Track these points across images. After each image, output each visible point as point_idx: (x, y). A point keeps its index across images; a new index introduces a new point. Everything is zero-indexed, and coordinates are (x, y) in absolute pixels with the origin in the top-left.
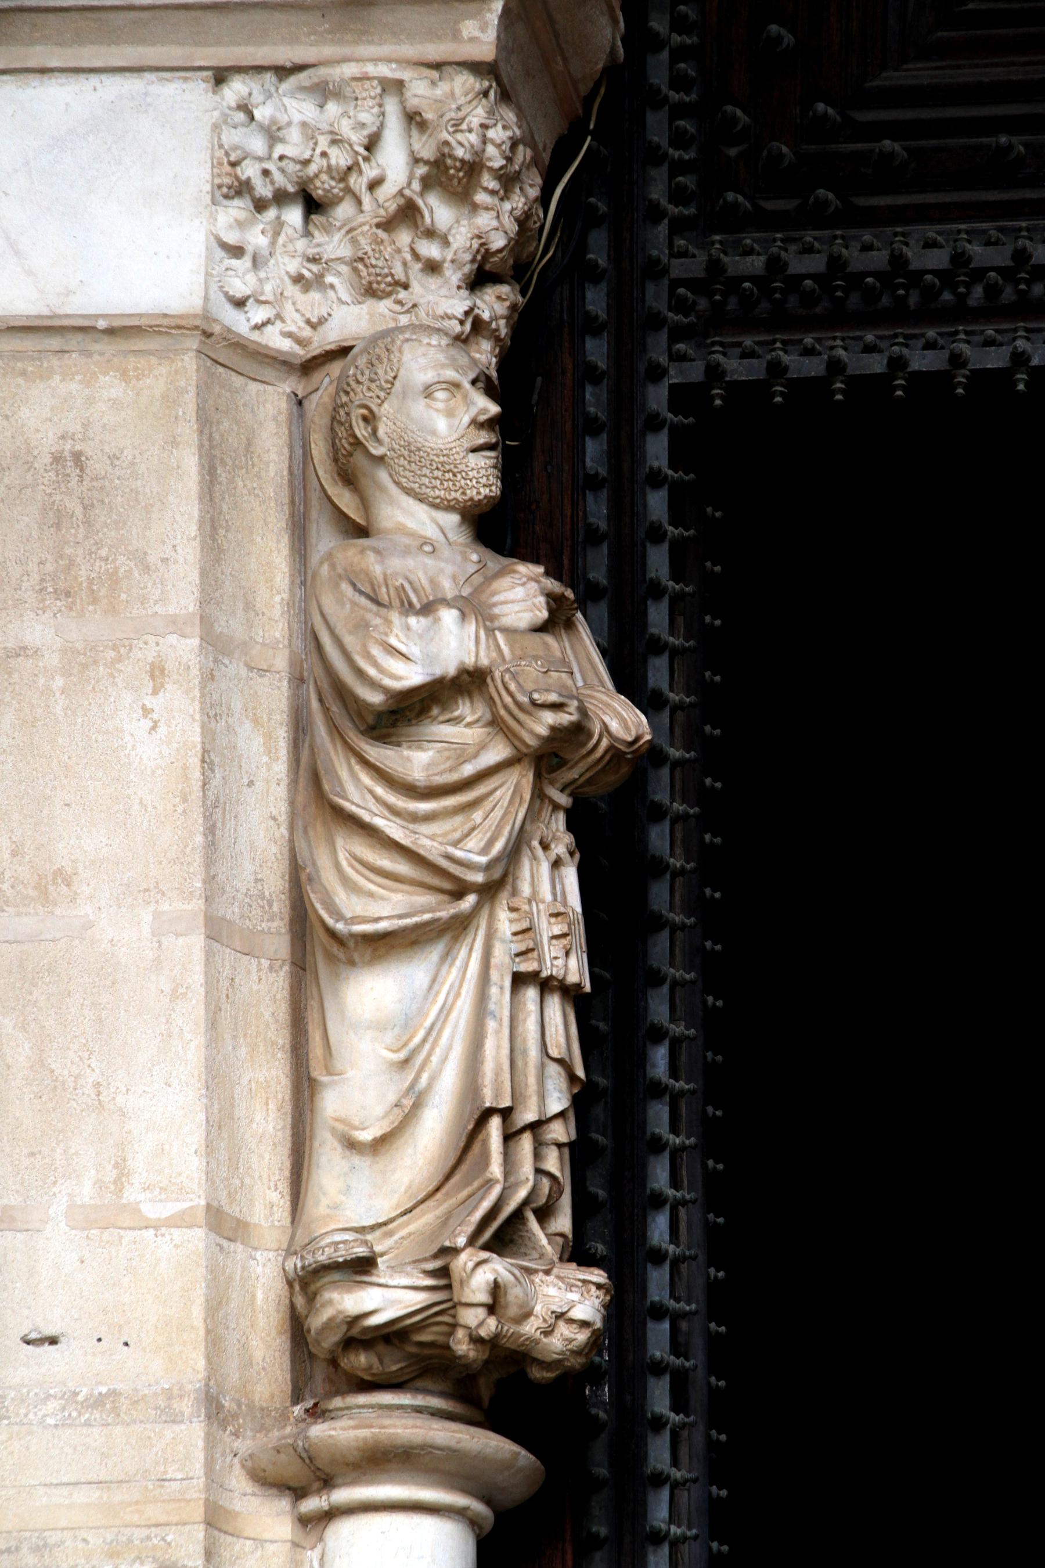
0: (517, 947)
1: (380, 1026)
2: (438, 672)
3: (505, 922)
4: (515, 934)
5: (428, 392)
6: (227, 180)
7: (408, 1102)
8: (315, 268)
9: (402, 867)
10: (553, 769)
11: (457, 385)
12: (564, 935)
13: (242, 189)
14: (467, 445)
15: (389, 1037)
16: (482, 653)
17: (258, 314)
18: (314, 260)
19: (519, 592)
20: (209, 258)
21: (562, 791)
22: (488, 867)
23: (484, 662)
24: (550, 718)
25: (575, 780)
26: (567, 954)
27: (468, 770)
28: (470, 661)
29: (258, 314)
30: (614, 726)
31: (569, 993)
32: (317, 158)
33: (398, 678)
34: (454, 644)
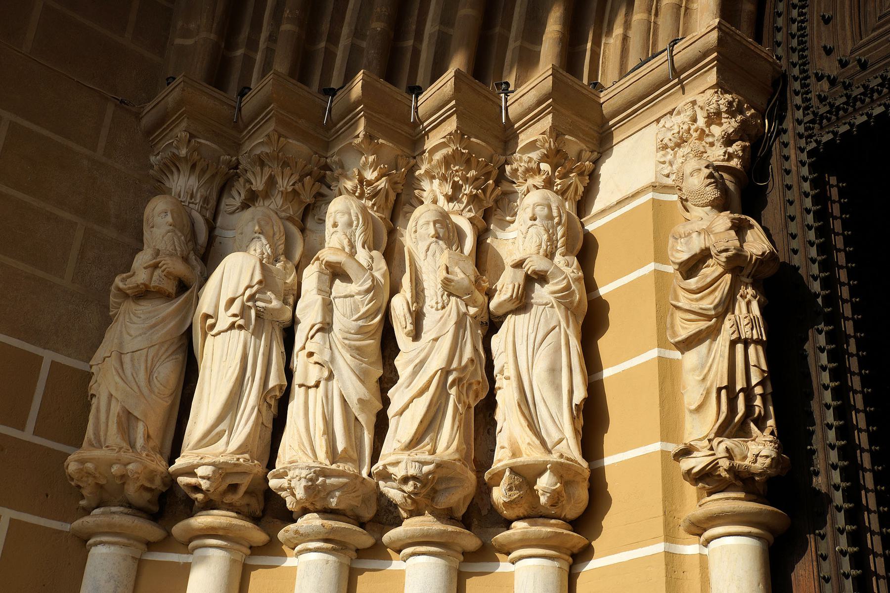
0: (731, 332)
1: (694, 370)
2: (693, 253)
3: (727, 324)
4: (731, 327)
5: (692, 175)
6: (661, 146)
7: (705, 393)
8: (684, 158)
9: (693, 317)
10: (741, 271)
11: (700, 170)
12: (748, 323)
13: (665, 147)
14: (704, 185)
15: (697, 372)
16: (706, 243)
17: (673, 177)
18: (683, 156)
19: (721, 221)
20: (656, 166)
21: (748, 278)
22: (715, 308)
23: (708, 245)
24: (725, 254)
25: (750, 273)
26: (752, 329)
27: (709, 280)
28: (703, 247)
29: (673, 177)
30: (754, 251)
31: (758, 342)
32: (681, 130)
33: (678, 259)
34: (697, 242)
